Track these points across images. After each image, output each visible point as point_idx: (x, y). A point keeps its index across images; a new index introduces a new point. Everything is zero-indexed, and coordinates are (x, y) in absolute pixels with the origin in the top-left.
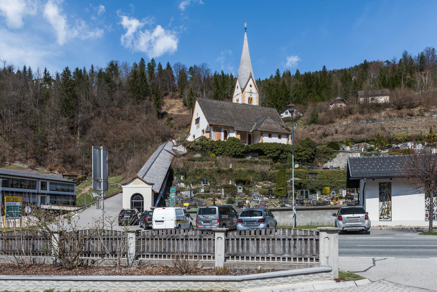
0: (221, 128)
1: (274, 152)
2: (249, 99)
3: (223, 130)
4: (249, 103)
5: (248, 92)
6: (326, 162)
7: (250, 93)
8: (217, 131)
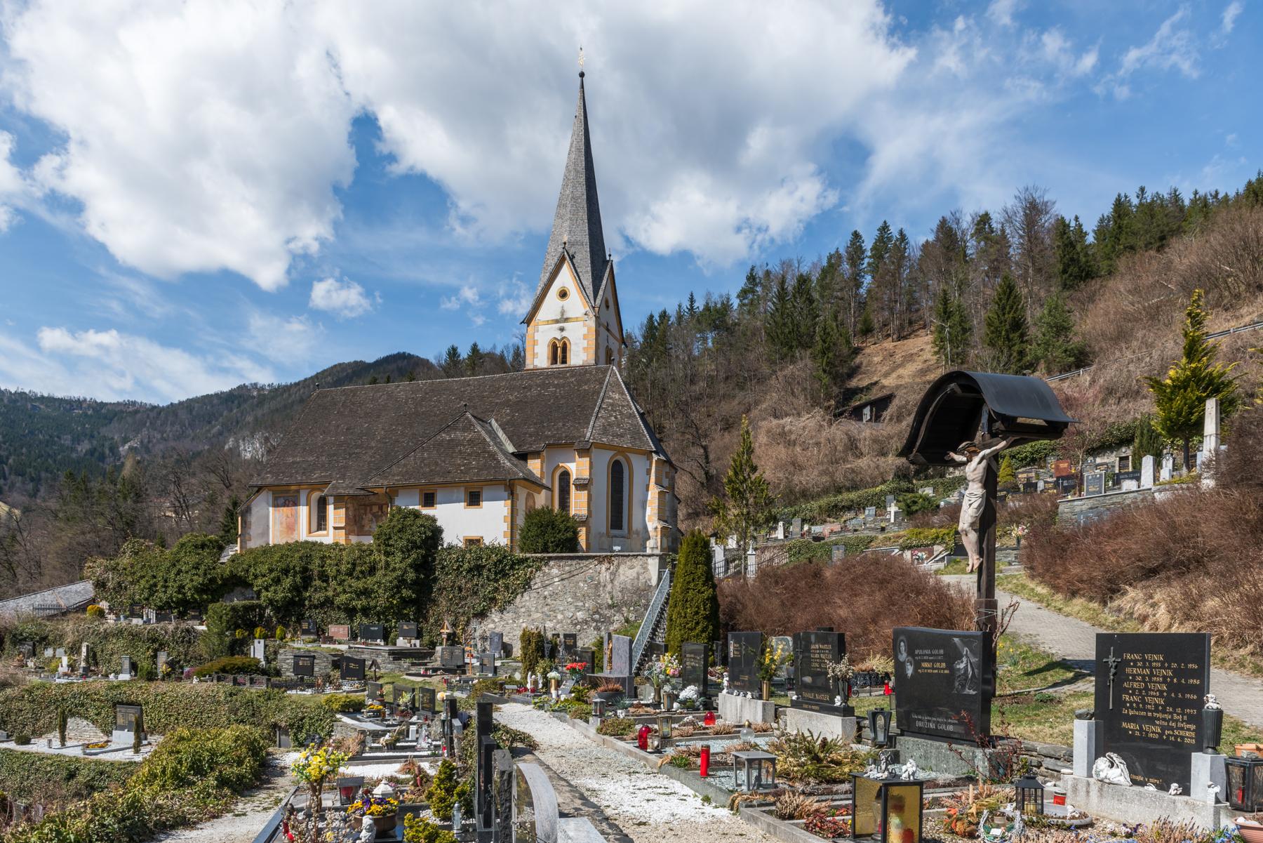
0: (298, 491)
1: (277, 581)
2: (554, 347)
3: (303, 498)
4: (554, 360)
5: (548, 322)
6: (482, 615)
7: (557, 321)
8: (285, 505)
